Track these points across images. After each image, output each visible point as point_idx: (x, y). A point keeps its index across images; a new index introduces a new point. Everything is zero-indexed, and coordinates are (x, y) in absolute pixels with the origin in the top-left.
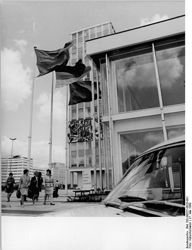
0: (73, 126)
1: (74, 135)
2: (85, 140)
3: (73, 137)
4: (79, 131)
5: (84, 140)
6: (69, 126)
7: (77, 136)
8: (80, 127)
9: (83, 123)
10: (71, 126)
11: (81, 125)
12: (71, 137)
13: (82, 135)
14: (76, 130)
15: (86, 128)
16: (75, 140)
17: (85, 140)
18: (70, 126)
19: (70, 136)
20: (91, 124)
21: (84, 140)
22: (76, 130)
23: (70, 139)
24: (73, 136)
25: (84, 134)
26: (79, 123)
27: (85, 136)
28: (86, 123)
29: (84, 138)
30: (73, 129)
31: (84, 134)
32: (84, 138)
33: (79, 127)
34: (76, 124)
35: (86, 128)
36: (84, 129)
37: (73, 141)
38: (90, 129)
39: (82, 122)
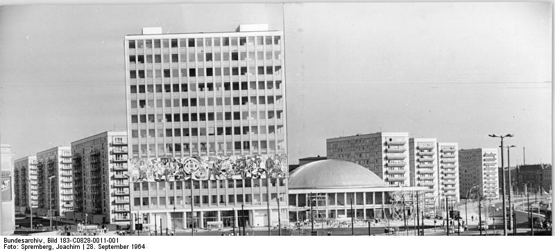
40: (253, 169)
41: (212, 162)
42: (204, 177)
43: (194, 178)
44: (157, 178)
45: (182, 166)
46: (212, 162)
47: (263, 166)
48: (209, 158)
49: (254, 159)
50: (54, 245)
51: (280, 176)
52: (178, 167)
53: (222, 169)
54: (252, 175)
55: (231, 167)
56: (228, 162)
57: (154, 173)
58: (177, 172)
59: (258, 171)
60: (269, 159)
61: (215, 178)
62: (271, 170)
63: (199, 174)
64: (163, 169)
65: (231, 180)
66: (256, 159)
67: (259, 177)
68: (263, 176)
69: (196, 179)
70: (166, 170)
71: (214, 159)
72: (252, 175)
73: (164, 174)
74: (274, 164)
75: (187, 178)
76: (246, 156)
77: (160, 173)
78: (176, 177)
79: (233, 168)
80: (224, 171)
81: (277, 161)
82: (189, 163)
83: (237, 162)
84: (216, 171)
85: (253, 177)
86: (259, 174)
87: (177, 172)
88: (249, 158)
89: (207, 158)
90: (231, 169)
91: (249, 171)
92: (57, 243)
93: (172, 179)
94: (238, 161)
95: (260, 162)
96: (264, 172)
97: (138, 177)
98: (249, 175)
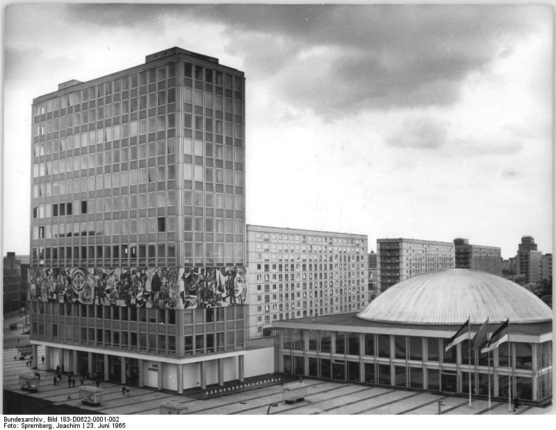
0: (190, 277)
1: (191, 296)
2: (207, 306)
3: (189, 300)
4: (198, 288)
5: (206, 305)
6: (182, 275)
7: (195, 297)
8: (201, 281)
9: (205, 274)
10: (186, 277)
11: (201, 276)
12: (186, 298)
13: (202, 297)
14: (194, 286)
15: (209, 283)
16: (193, 305)
17: (207, 306)
18: (183, 277)
19: (185, 296)
20: (215, 277)
21: (206, 305)
22: (194, 286)
23: (184, 302)
24: (189, 298)
25: (205, 295)
26: (197, 272)
27: (208, 297)
28: (208, 274)
29: (206, 303)
30: (189, 282)
31: (205, 295)
32: (206, 303)
33: (198, 281)
34: (194, 275)
35: (209, 283)
36: (207, 285)
37: (189, 308)
38: (214, 286)
39: (202, 270)
40: (137, 292)
41: (97, 277)
42: (89, 300)
43: (80, 300)
44: (50, 297)
45: (70, 280)
46: (97, 277)
47: (149, 288)
48: (95, 270)
49: (138, 274)
50: (54, 424)
51: (167, 305)
52: (67, 281)
53: (106, 289)
54: (137, 301)
55: (115, 287)
56: (112, 279)
57: (48, 288)
58: (66, 289)
59: (143, 295)
60: (156, 275)
61: (100, 302)
62: (157, 295)
63: (85, 294)
64: (55, 284)
65: (116, 308)
66: (142, 275)
67: (145, 303)
68: (149, 305)
69: (83, 303)
70: (57, 286)
71: (100, 272)
72: (137, 301)
73: (55, 292)
74: (161, 284)
75: (74, 300)
76: (131, 270)
77: (52, 291)
78: (65, 296)
79: (117, 288)
80: (108, 291)
81: (164, 280)
82: (76, 277)
83: (121, 278)
84: (100, 291)
85: (138, 306)
86: (145, 300)
87: (66, 289)
88: (134, 272)
89: (91, 271)
90: (116, 290)
91: (133, 294)
92: (57, 423)
93: (62, 301)
94: (123, 276)
95: (145, 280)
96: (150, 298)
97: (35, 295)
98: (133, 301)
